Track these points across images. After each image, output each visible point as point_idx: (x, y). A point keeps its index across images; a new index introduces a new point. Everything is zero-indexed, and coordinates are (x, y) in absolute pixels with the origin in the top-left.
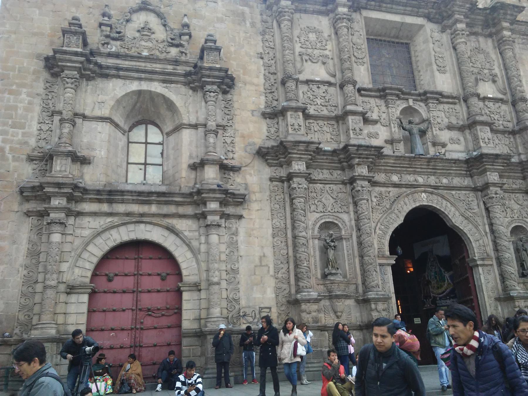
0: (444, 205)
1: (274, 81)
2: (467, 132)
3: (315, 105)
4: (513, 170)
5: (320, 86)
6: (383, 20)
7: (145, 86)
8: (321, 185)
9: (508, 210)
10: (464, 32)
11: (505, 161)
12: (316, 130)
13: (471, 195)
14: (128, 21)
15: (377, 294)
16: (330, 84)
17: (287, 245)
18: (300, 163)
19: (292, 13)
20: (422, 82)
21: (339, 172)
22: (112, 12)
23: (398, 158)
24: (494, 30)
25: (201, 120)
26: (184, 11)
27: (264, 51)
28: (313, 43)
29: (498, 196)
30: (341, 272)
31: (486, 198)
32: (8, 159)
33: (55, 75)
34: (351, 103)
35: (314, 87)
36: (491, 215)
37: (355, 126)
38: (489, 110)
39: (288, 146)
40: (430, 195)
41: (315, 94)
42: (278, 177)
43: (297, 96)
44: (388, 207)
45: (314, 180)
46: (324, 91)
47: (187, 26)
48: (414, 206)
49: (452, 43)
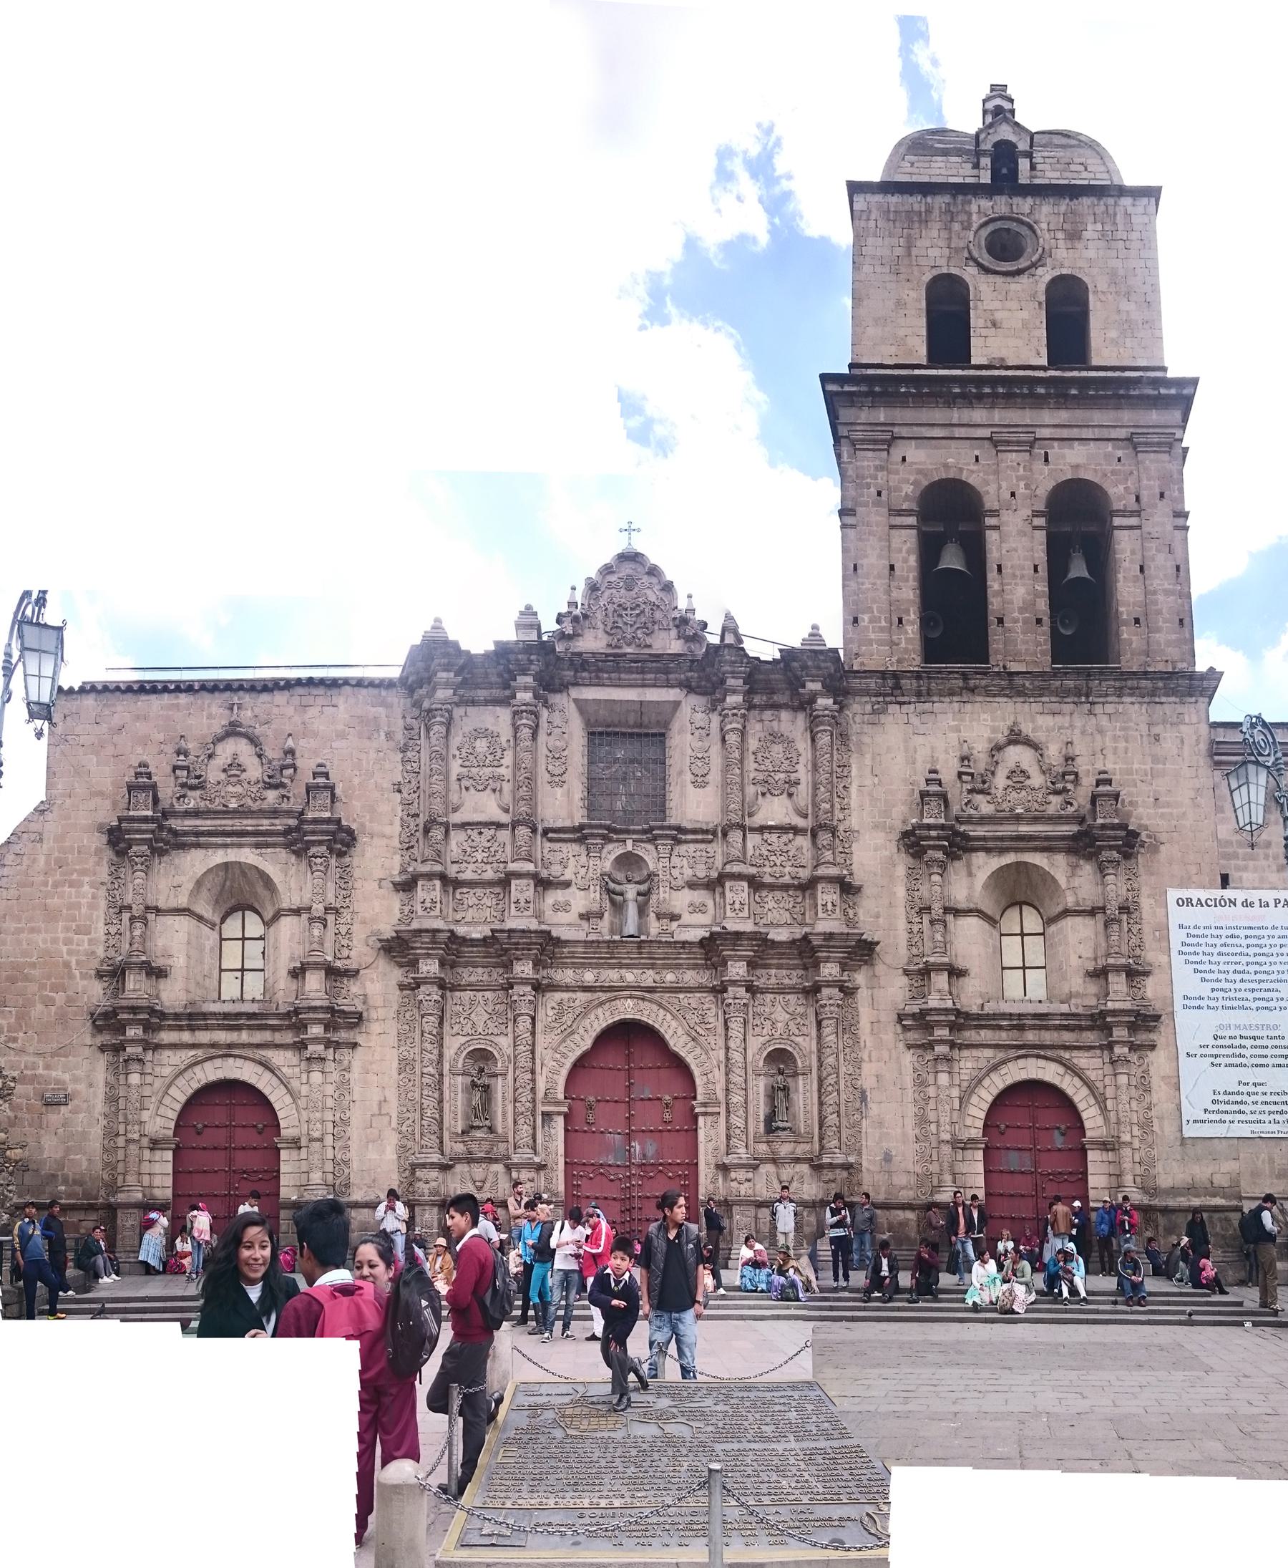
7: (232, 855)
14: (210, 756)
21: (501, 971)
22: (190, 746)
25: (306, 902)
26: (288, 729)
32: (75, 977)
33: (121, 854)
47: (291, 752)
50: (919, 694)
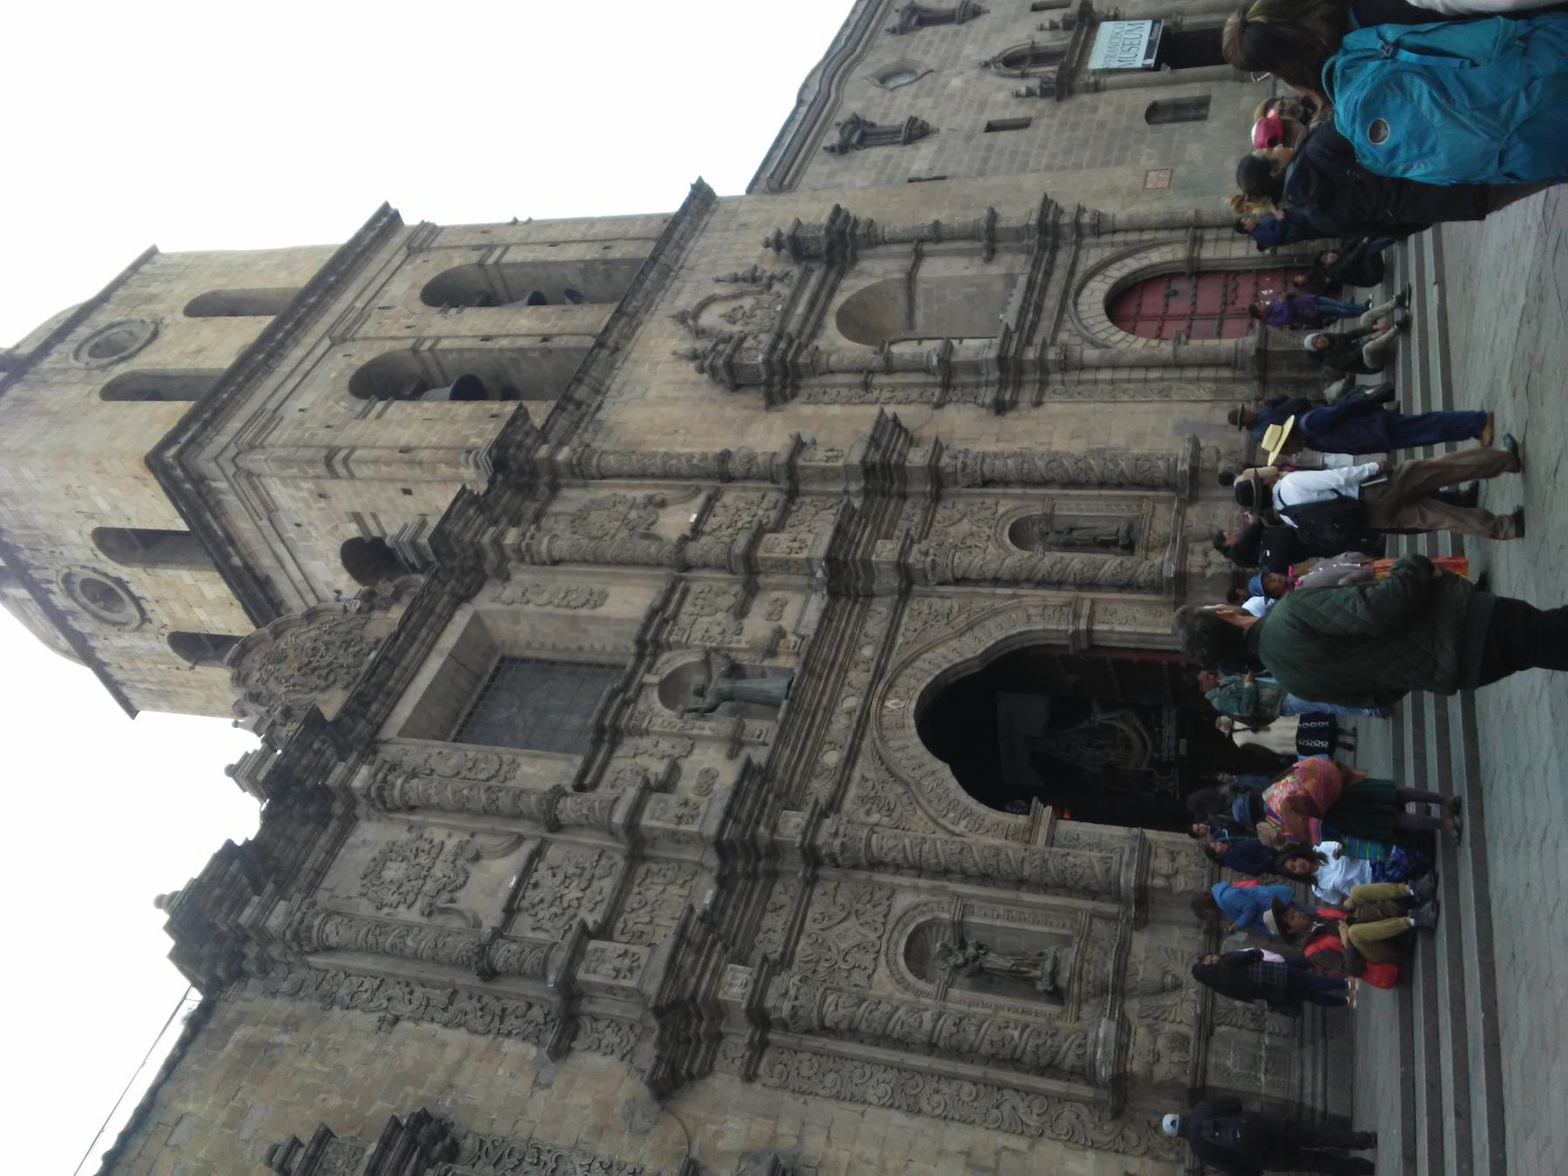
0: (927, 667)
1: (474, 1001)
2: (762, 580)
3: (579, 906)
4: (877, 513)
5: (532, 881)
6: (425, 696)
8: (802, 943)
9: (969, 542)
10: (529, 534)
11: (856, 519)
12: (646, 919)
13: (916, 607)
15: (1128, 865)
16: (537, 855)
17: (951, 1077)
18: (727, 978)
19: (314, 904)
20: (609, 648)
21: (778, 888)
23: (782, 737)
24: (546, 478)
27: (378, 1009)
28: (413, 872)
29: (931, 551)
30: (1053, 948)
31: (930, 577)
34: (607, 811)
35: (532, 896)
36: (973, 576)
37: (671, 814)
38: (724, 527)
39: (673, 996)
40: (894, 690)
41: (549, 898)
42: (748, 1054)
43: (536, 946)
44: (901, 790)
45: (783, 955)
46: (550, 872)
48: (914, 731)
49: (543, 563)
50: (597, 392)
